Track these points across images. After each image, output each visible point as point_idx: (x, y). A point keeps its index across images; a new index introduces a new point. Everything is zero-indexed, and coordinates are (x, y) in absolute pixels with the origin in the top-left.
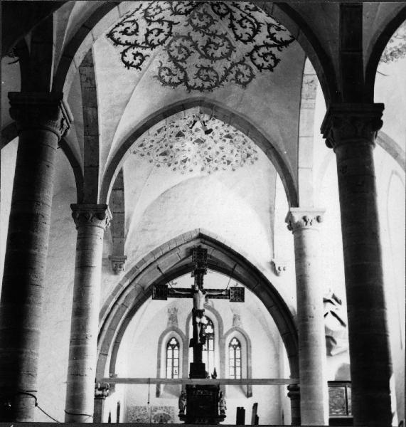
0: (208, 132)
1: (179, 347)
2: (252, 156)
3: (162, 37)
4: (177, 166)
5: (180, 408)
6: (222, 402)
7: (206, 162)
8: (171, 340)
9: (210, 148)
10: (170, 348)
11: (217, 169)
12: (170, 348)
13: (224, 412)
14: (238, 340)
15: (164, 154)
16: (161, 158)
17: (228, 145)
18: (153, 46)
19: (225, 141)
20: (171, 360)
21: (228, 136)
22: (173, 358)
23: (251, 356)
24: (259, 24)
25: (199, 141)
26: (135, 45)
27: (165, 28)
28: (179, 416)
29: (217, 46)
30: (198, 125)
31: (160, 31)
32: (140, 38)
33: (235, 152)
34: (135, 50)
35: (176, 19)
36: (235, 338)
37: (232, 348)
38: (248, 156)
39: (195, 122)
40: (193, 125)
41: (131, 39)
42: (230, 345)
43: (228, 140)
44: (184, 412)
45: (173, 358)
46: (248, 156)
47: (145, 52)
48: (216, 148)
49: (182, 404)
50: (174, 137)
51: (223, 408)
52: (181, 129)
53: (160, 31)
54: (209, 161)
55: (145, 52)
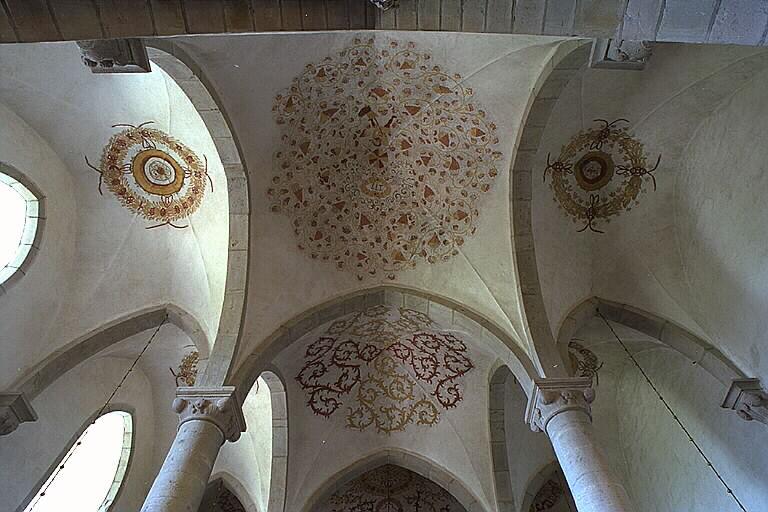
0: (367, 110)
2: (283, 107)
3: (424, 339)
4: (421, 63)
7: (364, 57)
9: (360, 83)
11: (342, 54)
15: (447, 90)
16: (450, 85)
17: (329, 97)
18: (434, 337)
19: (335, 104)
21: (332, 112)
24: (334, 362)
25: (380, 92)
26: (450, 349)
27: (420, 344)
29: (368, 330)
30: (383, 120)
31: (425, 343)
32: (443, 350)
33: (314, 94)
34: (451, 345)
35: (409, 344)
38: (289, 103)
39: (387, 126)
40: (391, 121)
41: (451, 353)
43: (330, 106)
46: (289, 103)
47: (443, 338)
48: (351, 88)
50: (426, 107)
52: (412, 119)
53: (425, 343)
54: (360, 62)
55: (443, 338)
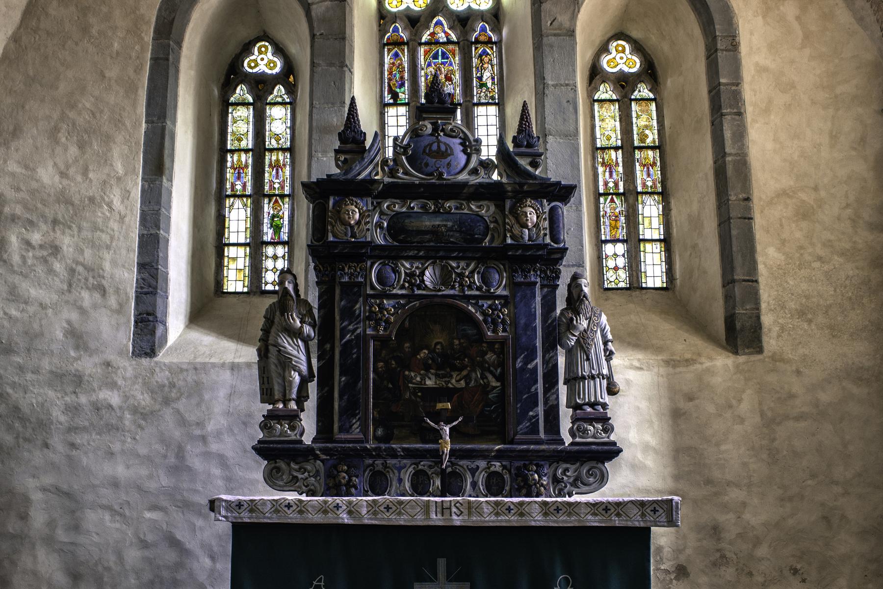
1: (291, 90)
5: (267, 395)
6: (583, 344)
8: (247, 49)
10: (241, 92)
12: (241, 92)
13: (604, 420)
14: (638, 48)
20: (247, 159)
22: (259, 150)
23: (737, 98)
28: (263, 450)
36: (619, 36)
37: (605, 92)
42: (595, 74)
44: (293, 418)
45: (259, 150)
49: (286, 363)
51: (596, 391)
